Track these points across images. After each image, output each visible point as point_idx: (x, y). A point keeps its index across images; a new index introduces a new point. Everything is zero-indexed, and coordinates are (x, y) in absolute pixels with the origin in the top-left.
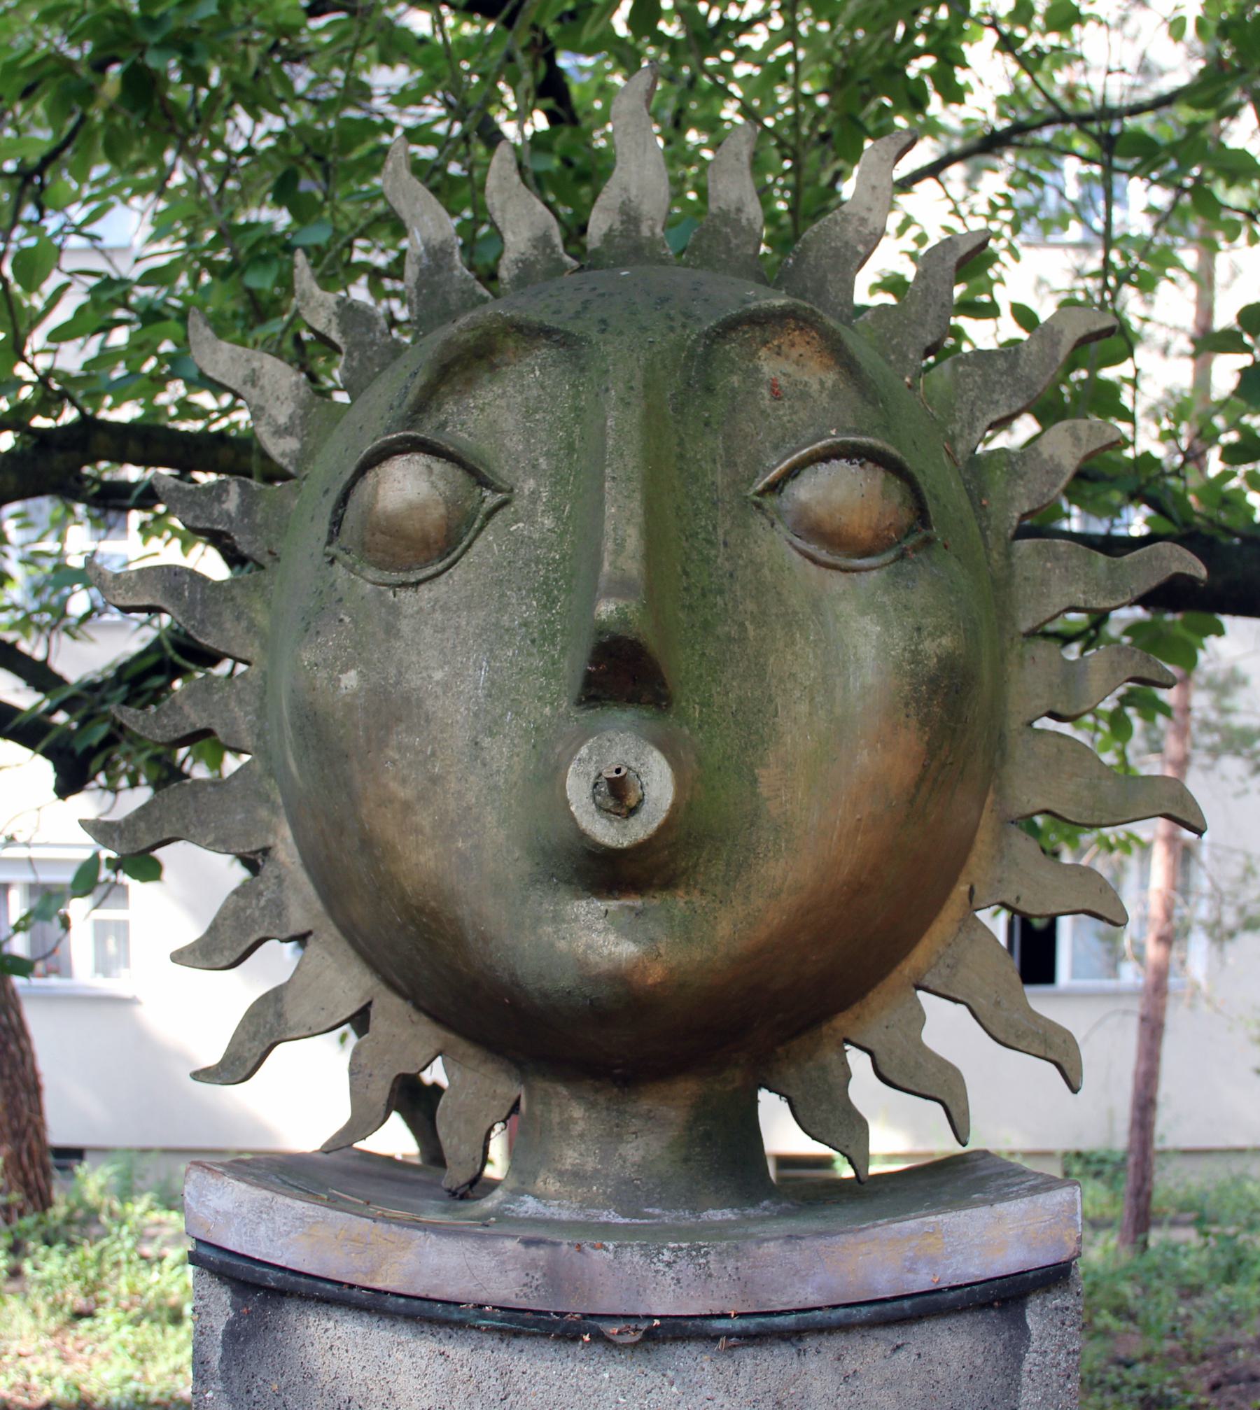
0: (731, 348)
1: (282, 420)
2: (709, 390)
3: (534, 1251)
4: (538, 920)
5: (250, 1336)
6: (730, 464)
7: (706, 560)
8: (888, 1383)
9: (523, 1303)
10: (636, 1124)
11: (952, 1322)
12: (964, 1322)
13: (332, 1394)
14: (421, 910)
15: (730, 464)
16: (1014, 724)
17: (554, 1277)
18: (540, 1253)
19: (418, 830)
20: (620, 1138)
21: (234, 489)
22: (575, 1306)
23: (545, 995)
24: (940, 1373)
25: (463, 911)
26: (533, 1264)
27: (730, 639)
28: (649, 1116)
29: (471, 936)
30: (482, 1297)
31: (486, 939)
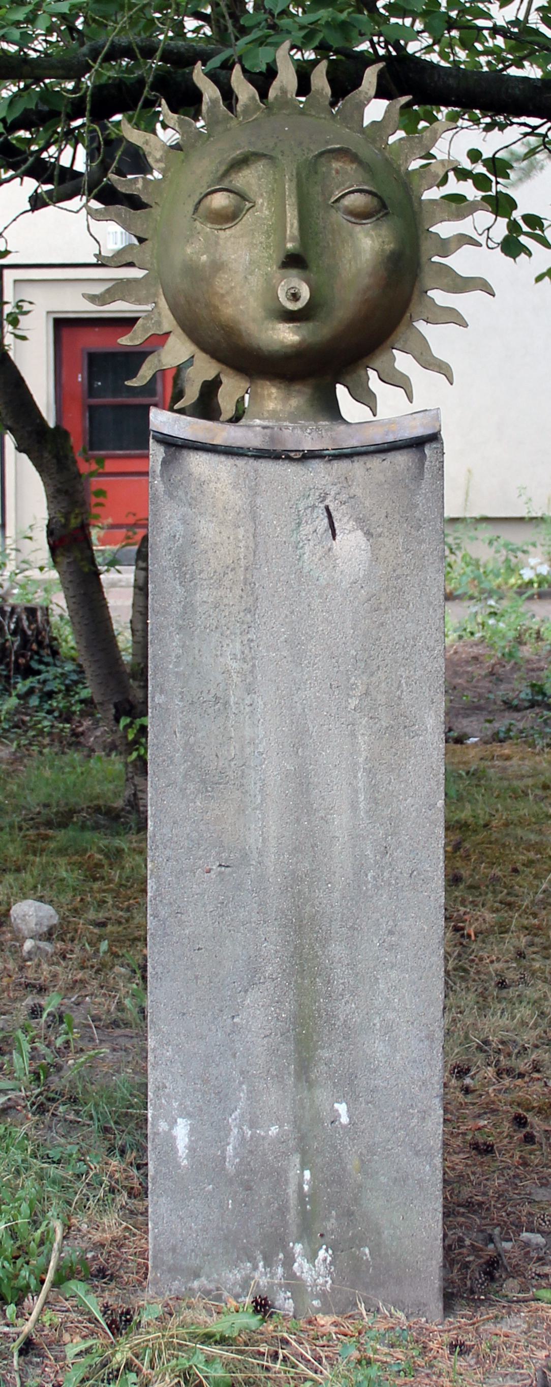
0: (323, 160)
1: (158, 157)
2: (316, 173)
3: (266, 430)
4: (267, 329)
5: (170, 462)
6: (323, 194)
7: (317, 224)
8: (381, 471)
9: (262, 447)
10: (294, 394)
11: (401, 452)
12: (405, 452)
13: (199, 479)
14: (227, 326)
15: (323, 194)
16: (424, 259)
17: (272, 439)
18: (268, 431)
19: (227, 303)
20: (289, 399)
21: (140, 181)
22: (279, 448)
23: (270, 352)
24: (398, 468)
25: (242, 327)
26: (266, 435)
27: (325, 247)
28: (299, 391)
29: (244, 334)
30: (249, 445)
31: (249, 335)
